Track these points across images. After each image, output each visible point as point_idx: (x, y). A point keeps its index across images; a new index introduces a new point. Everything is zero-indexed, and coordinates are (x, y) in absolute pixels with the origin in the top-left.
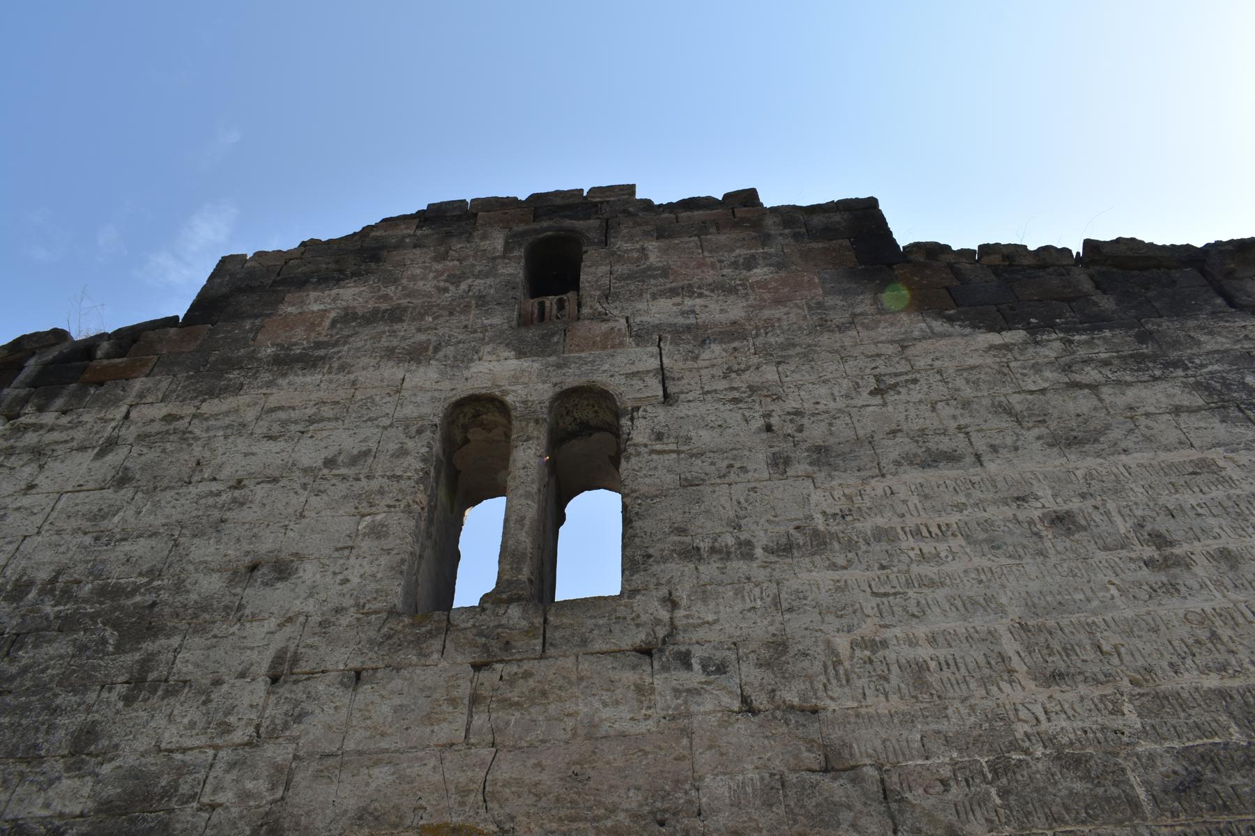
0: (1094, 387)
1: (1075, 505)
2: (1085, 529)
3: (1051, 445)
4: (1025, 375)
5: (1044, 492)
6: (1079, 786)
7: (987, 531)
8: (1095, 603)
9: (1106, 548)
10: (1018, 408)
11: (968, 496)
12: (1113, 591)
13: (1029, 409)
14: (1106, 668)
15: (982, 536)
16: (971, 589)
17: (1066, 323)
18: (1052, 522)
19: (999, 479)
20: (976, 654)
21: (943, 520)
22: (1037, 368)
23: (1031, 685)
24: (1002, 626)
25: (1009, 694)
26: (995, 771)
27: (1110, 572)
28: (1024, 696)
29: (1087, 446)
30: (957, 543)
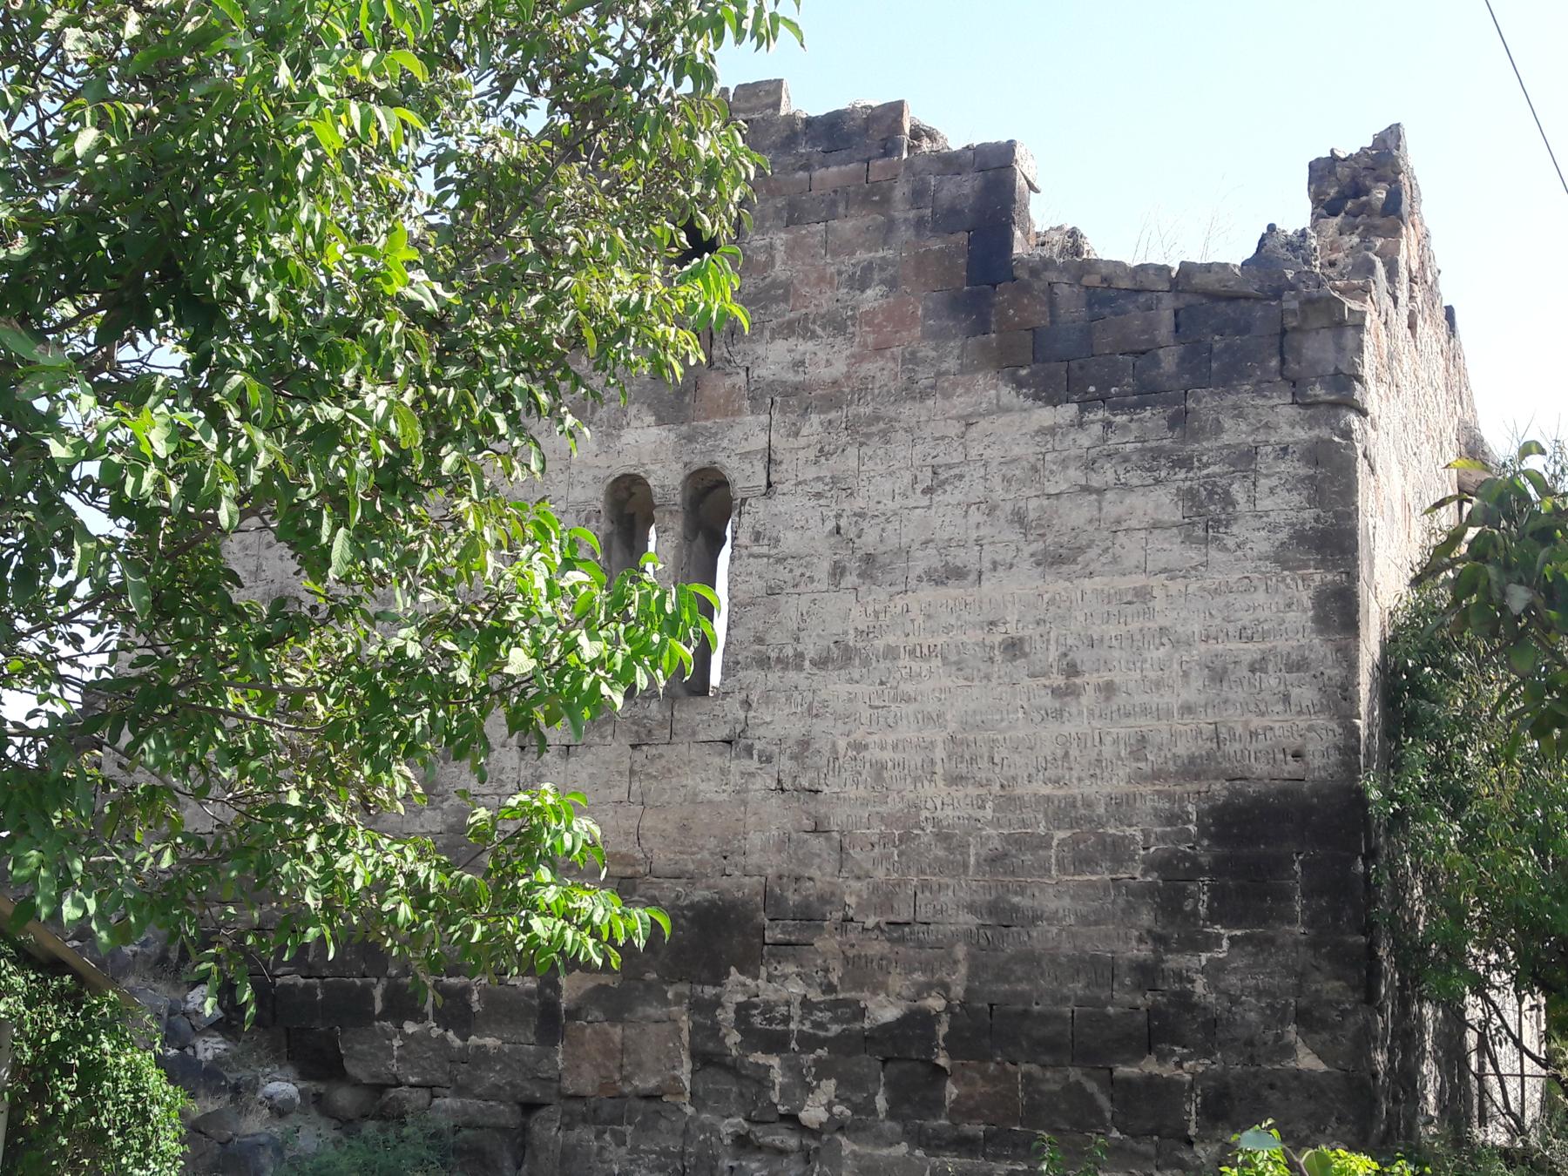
0: (1100, 492)
1: (1026, 633)
2: (1025, 655)
3: (1038, 564)
4: (1052, 472)
5: (1012, 618)
6: (941, 853)
7: (959, 653)
8: (1004, 724)
9: (1032, 675)
10: (1032, 515)
11: (958, 618)
12: (1020, 715)
13: (1039, 518)
14: (991, 775)
15: (953, 658)
16: (932, 707)
17: (1117, 395)
18: (1006, 649)
19: (986, 600)
20: (916, 759)
21: (931, 641)
22: (1064, 464)
23: (941, 784)
24: (940, 736)
25: (927, 789)
26: (901, 840)
27: (1025, 698)
28: (934, 792)
29: (1065, 568)
30: (936, 662)
